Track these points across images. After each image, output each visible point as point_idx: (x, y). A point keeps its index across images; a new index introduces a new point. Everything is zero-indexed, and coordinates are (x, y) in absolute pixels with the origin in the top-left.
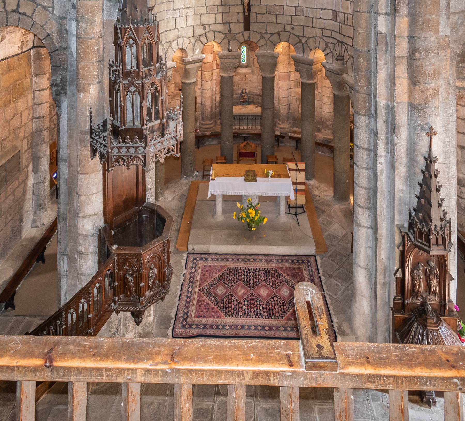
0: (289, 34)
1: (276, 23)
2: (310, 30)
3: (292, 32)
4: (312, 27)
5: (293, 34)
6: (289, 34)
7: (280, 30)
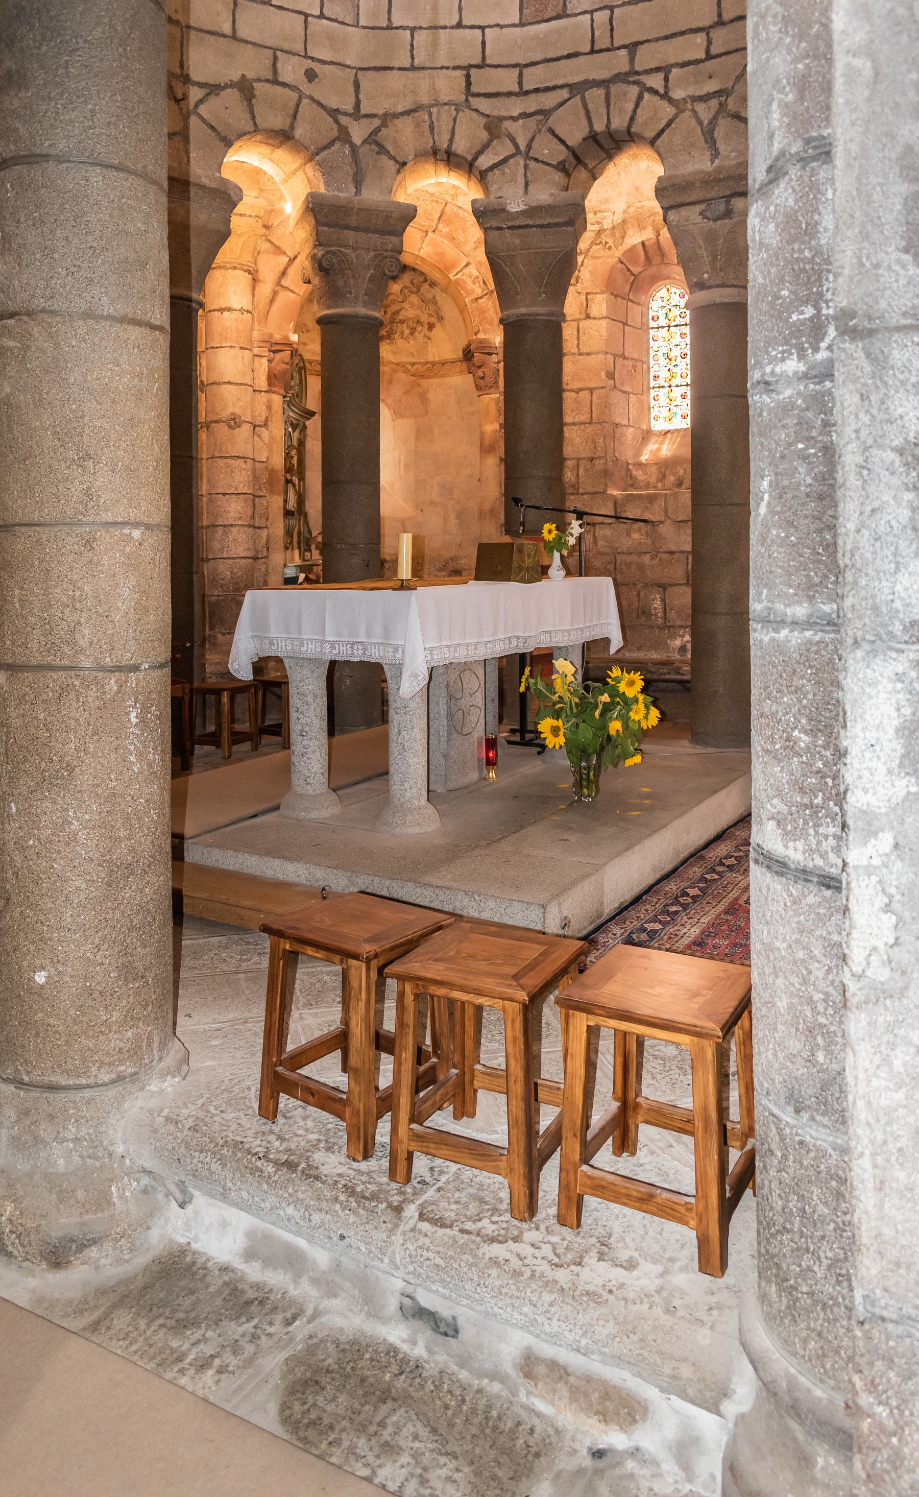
0: (295, 96)
1: (234, 37)
2: (395, 81)
3: (306, 88)
4: (413, 68)
5: (311, 98)
6: (295, 96)
7: (250, 75)
